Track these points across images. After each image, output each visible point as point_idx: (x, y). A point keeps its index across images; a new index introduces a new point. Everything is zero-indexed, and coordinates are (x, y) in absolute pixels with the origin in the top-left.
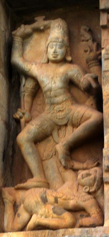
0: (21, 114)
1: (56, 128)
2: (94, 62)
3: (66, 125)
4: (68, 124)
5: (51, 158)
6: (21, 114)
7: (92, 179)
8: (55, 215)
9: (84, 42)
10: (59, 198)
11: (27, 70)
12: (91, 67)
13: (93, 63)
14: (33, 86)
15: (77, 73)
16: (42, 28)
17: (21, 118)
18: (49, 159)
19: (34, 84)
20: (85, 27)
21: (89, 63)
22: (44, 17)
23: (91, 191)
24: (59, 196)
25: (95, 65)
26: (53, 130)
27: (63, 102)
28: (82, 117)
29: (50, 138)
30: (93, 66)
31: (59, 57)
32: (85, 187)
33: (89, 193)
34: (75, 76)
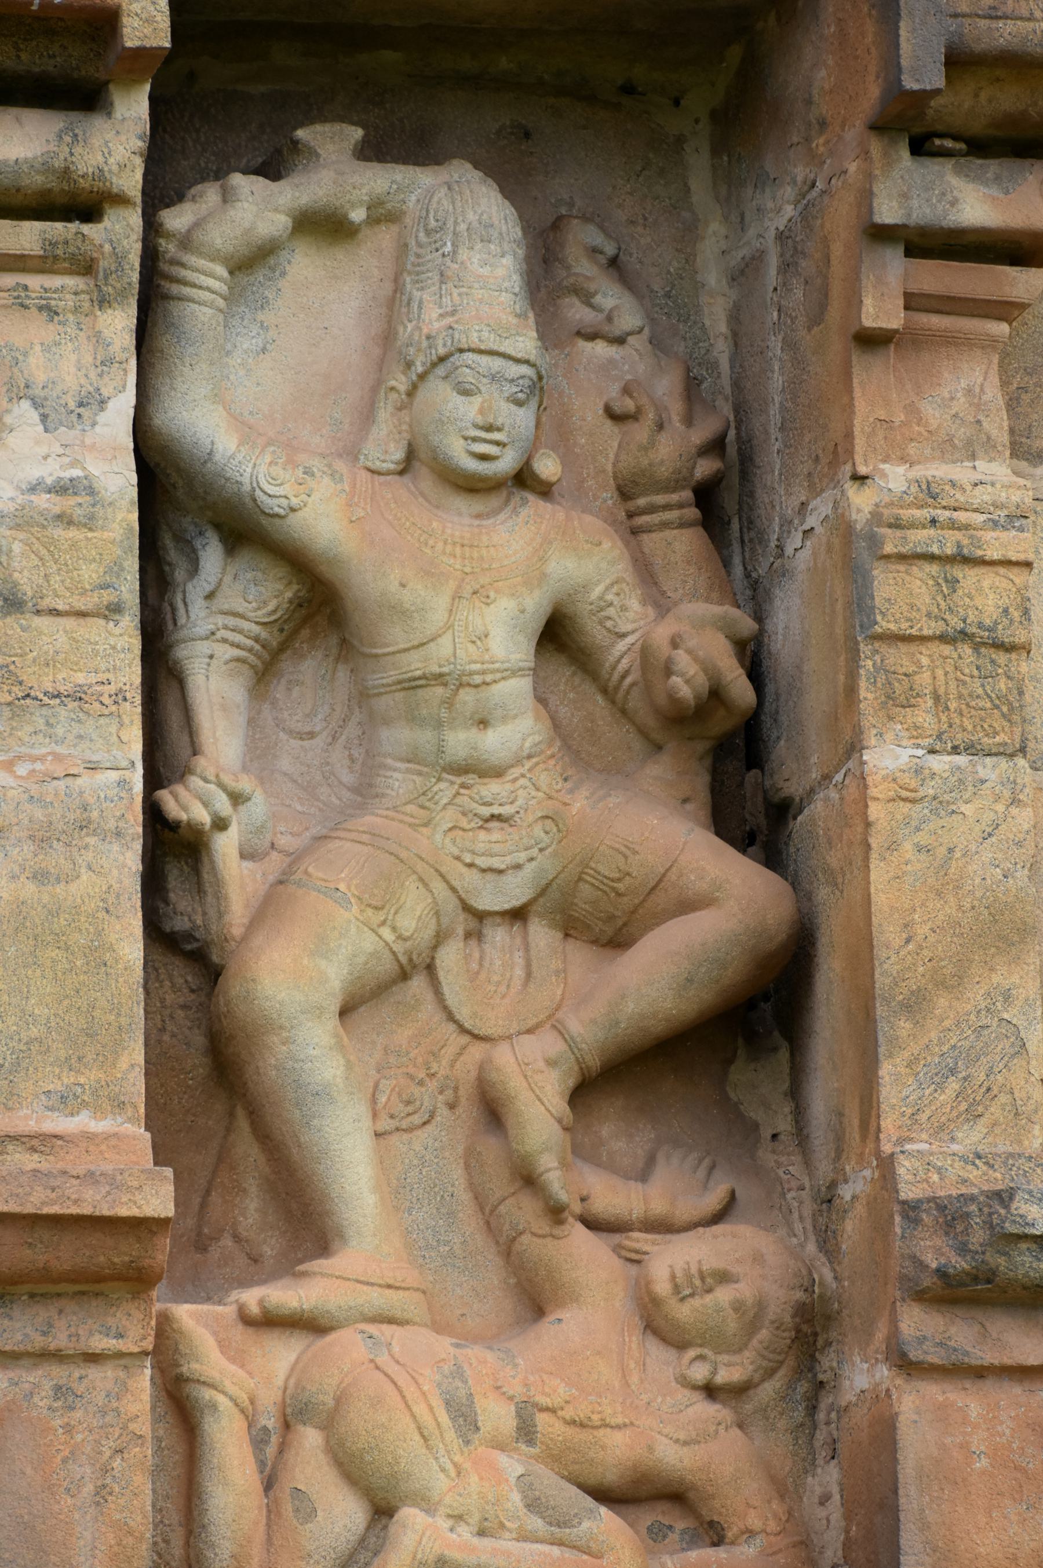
0: (223, 804)
1: (461, 923)
2: (675, 497)
3: (518, 915)
4: (534, 908)
5: (425, 1124)
6: (223, 804)
7: (738, 1306)
8: (536, 1523)
9: (600, 348)
10: (547, 1409)
11: (275, 506)
12: (649, 530)
13: (667, 507)
14: (274, 611)
15: (608, 581)
16: (358, 215)
17: (221, 824)
18: (409, 1130)
19: (289, 594)
20: (592, 235)
21: (642, 502)
22: (358, 133)
23: (722, 1377)
24: (544, 1401)
25: (682, 525)
26: (439, 939)
27: (518, 762)
28: (654, 888)
29: (418, 984)
30: (665, 525)
31: (507, 463)
32: (692, 1353)
33: (710, 1391)
34: (598, 590)
